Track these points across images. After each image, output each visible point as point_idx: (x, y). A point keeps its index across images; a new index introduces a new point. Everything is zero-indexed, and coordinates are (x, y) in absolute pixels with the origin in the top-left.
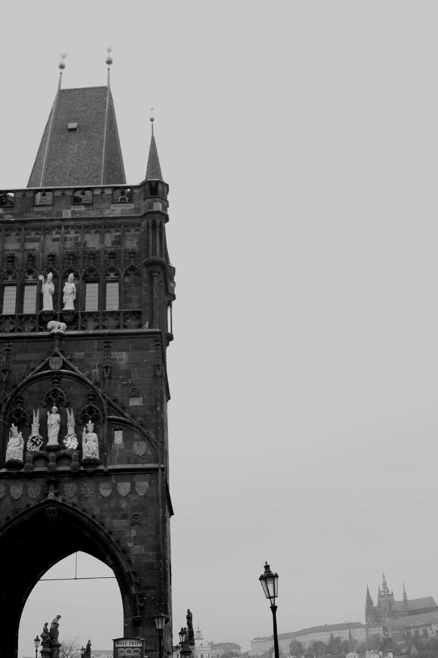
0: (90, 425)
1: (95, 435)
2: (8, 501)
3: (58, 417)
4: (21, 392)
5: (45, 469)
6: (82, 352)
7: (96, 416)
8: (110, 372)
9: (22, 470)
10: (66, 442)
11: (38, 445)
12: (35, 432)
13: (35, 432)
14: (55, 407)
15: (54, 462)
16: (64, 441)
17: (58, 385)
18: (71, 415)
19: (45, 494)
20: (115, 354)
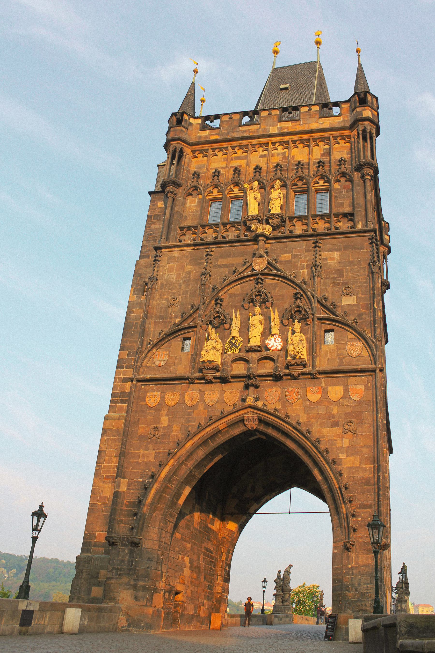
0: (297, 326)
1: (302, 334)
2: (201, 407)
3: (261, 317)
4: (222, 295)
5: (244, 372)
6: (289, 253)
7: (304, 315)
8: (320, 271)
9: (218, 374)
10: (269, 342)
11: (237, 347)
12: (235, 333)
13: (235, 333)
14: (257, 308)
15: (255, 364)
16: (267, 341)
17: (262, 285)
18: (275, 315)
19: (242, 399)
20: (324, 254)
